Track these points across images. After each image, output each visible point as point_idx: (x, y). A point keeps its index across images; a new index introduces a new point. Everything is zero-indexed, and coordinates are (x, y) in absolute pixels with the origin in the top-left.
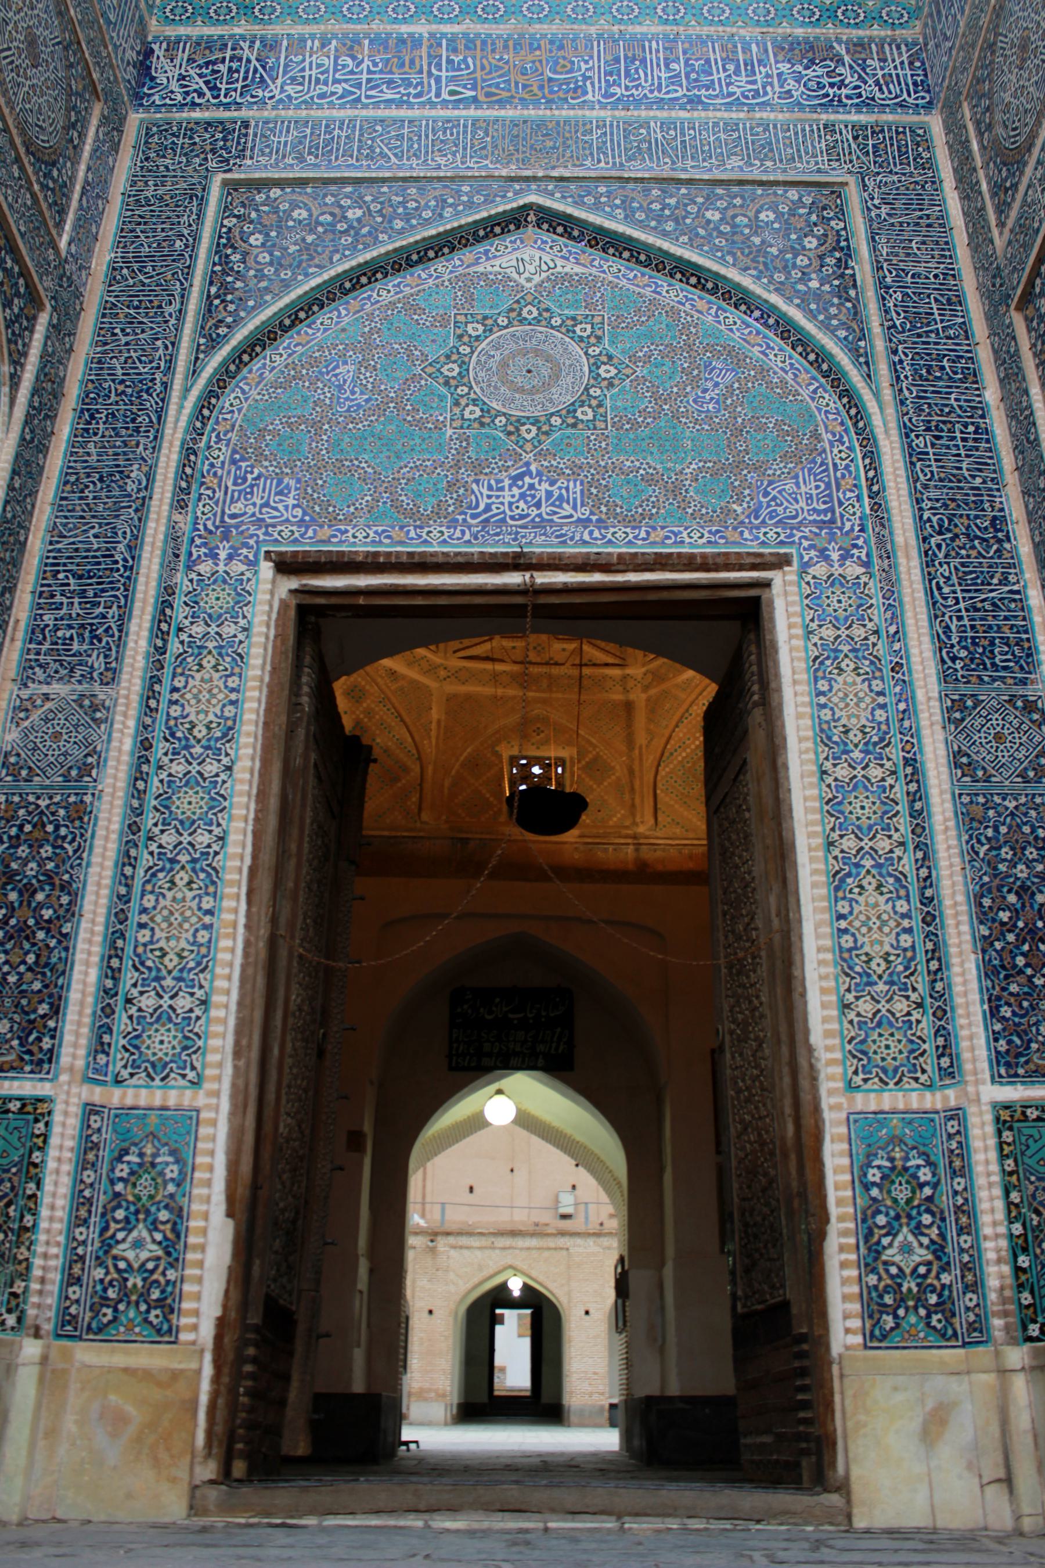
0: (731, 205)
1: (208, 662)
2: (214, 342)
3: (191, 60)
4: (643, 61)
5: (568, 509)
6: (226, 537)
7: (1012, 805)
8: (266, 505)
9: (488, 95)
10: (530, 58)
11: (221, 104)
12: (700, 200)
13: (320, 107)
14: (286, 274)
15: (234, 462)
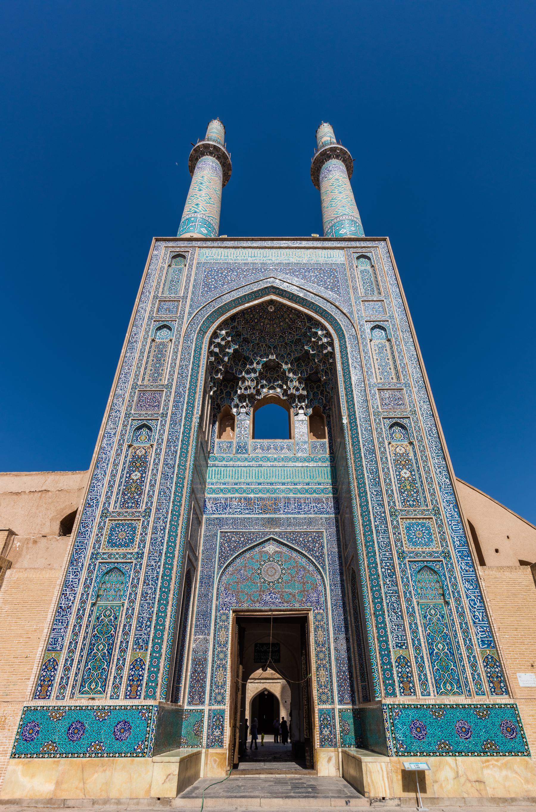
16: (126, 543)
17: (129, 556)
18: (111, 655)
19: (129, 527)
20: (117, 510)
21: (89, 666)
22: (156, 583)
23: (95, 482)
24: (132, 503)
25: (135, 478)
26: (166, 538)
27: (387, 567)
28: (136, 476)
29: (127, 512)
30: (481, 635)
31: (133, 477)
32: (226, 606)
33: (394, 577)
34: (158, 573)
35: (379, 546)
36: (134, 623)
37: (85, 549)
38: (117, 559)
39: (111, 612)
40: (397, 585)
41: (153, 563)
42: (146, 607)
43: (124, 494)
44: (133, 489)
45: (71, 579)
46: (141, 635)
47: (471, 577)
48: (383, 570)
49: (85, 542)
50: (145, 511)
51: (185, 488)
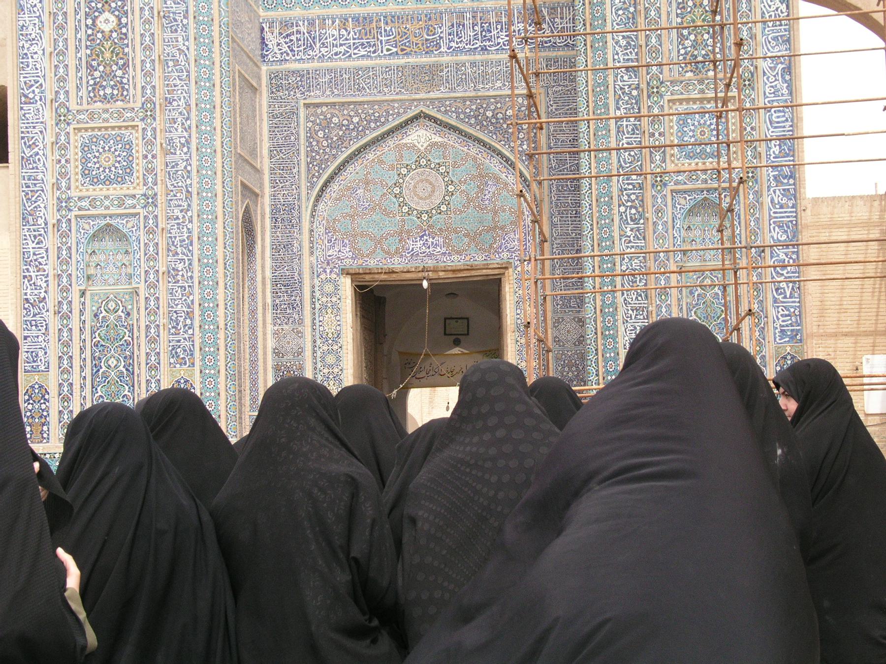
0: (496, 108)
1: (329, 311)
2: (312, 186)
3: (281, 34)
4: (463, 26)
5: (439, 249)
6: (328, 264)
7: (569, 353)
8: (340, 251)
9: (402, 50)
10: (418, 27)
11: (296, 60)
12: (485, 106)
13: (336, 60)
14: (334, 152)
15: (326, 233)
16: (117, 175)
17: (130, 202)
18: (133, 374)
19: (117, 143)
20: (85, 106)
21: (100, 393)
22: (190, 251)
23: (27, 45)
24: (113, 89)
25: (107, 28)
26: (194, 163)
27: (629, 204)
28: (107, 22)
29: (107, 111)
30: (783, 321)
31: (101, 25)
32: (332, 265)
33: (642, 221)
34: (190, 231)
35: (619, 161)
36: (162, 320)
37: (43, 191)
38: (107, 208)
39: (117, 304)
40: (644, 238)
41: (177, 213)
42: (179, 294)
43: (90, 66)
44: (108, 55)
45: (32, 251)
46: (179, 341)
47: (788, 217)
48: (622, 209)
49: (39, 177)
50: (142, 107)
51: (217, 44)
